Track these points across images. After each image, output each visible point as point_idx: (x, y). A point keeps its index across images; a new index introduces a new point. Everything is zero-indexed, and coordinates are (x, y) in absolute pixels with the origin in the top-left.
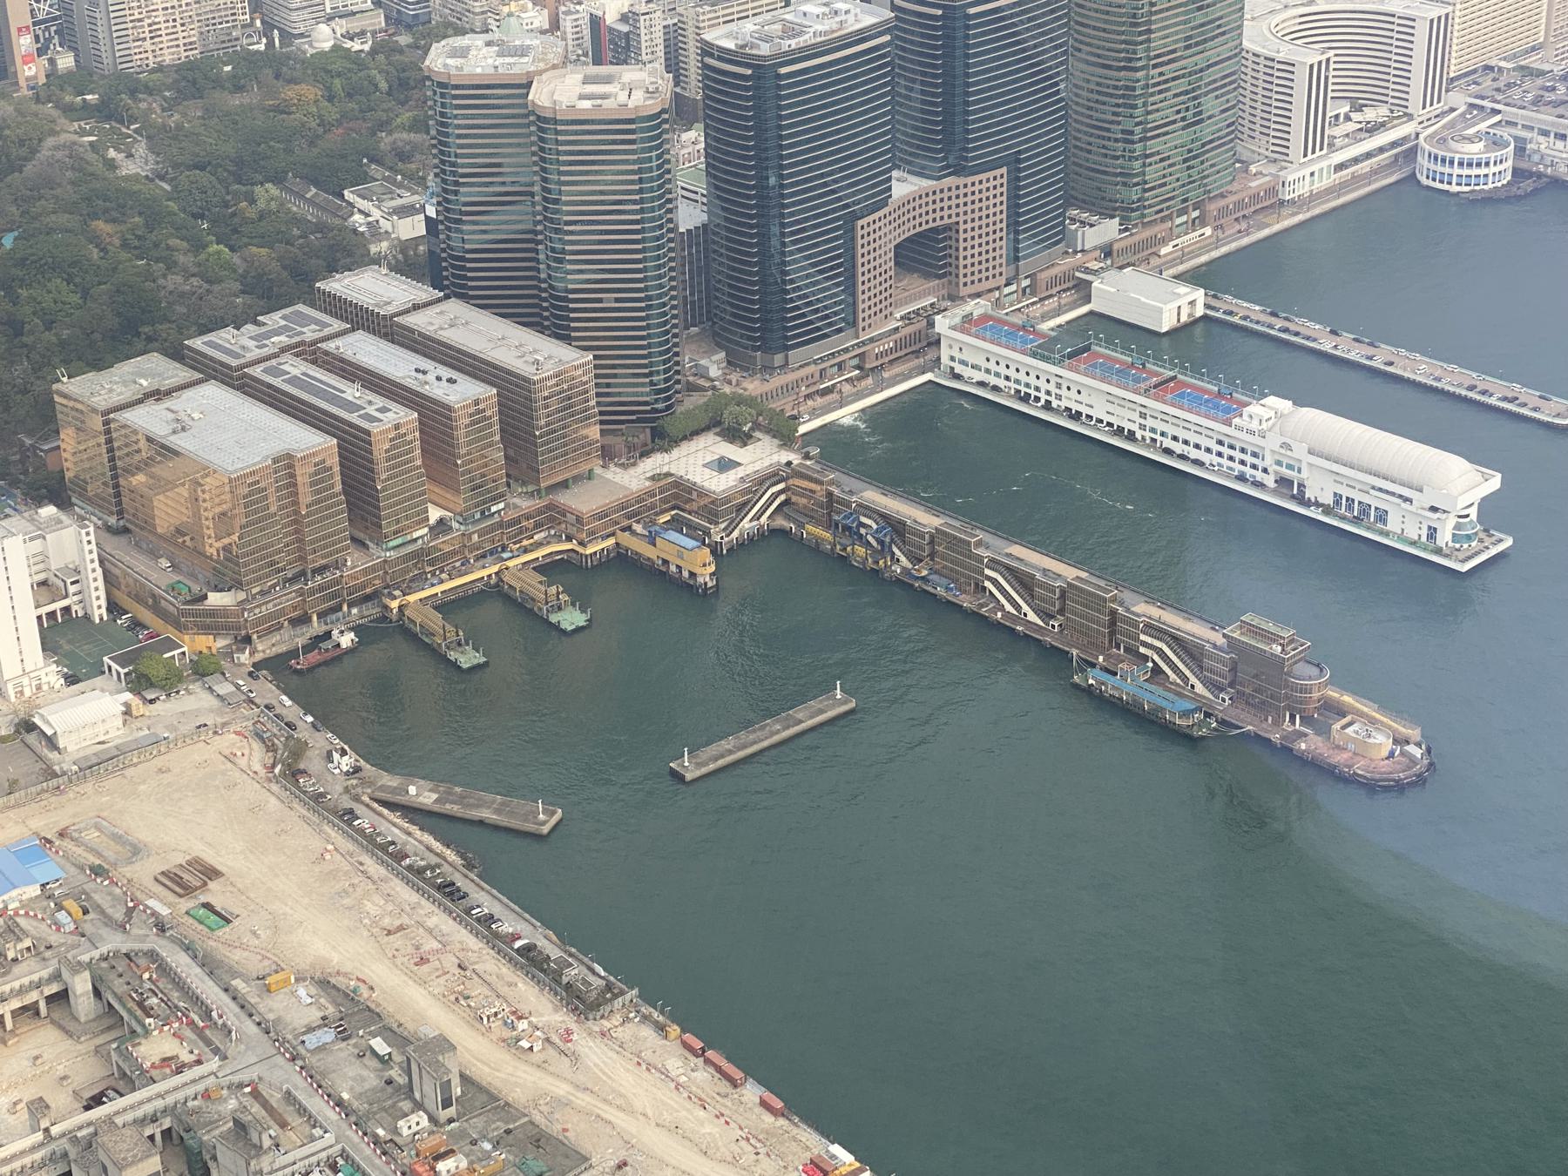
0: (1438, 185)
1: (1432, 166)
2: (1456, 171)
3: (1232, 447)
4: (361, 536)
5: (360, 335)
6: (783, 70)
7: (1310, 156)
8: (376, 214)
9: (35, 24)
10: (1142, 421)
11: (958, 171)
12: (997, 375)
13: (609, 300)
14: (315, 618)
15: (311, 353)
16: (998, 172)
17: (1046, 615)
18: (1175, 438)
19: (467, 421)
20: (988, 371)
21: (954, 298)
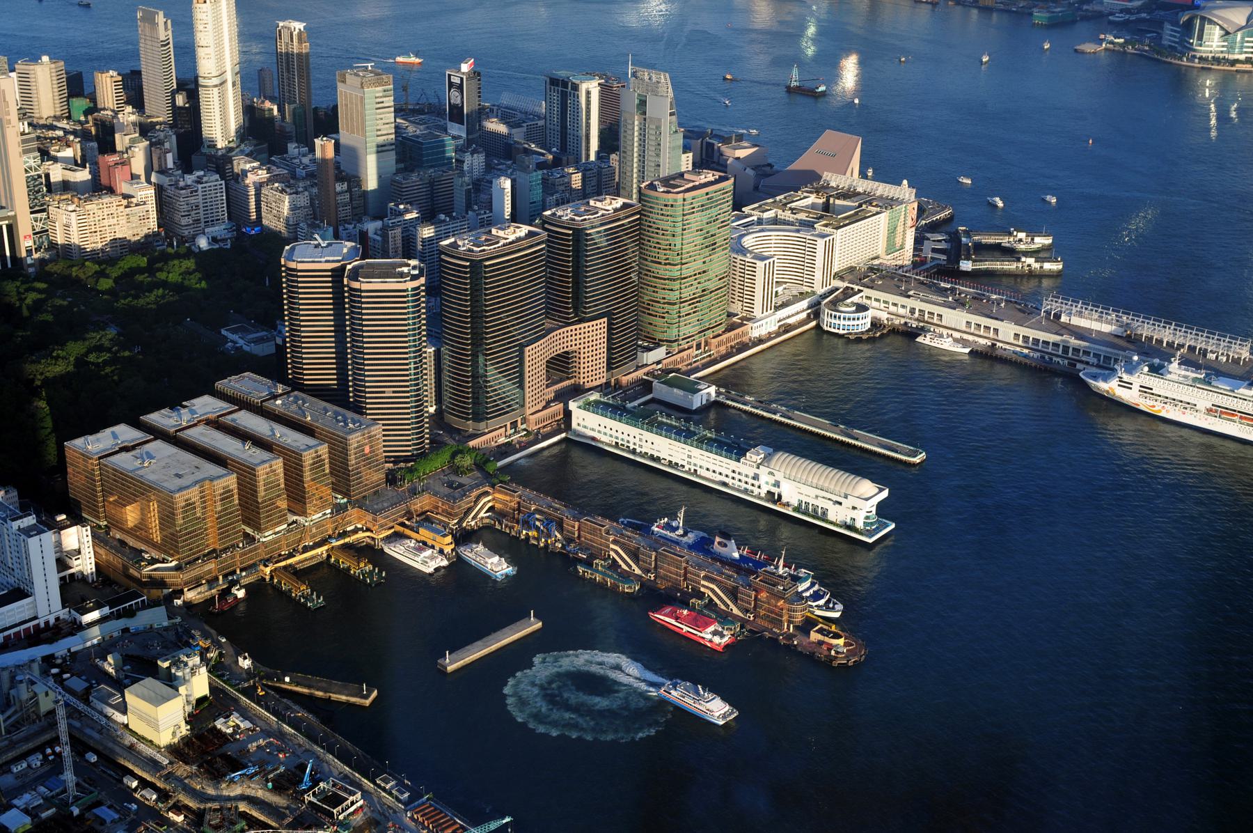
0: (832, 330)
1: (829, 320)
2: (842, 322)
3: (739, 473)
4: (249, 530)
5: (243, 412)
6: (487, 263)
7: (765, 313)
8: (241, 342)
9: (34, 234)
10: (689, 460)
11: (581, 321)
12: (605, 434)
13: (389, 392)
14: (221, 577)
15: (216, 424)
16: (602, 320)
17: (647, 571)
18: (708, 469)
19: (311, 461)
20: (599, 432)
21: (577, 391)
